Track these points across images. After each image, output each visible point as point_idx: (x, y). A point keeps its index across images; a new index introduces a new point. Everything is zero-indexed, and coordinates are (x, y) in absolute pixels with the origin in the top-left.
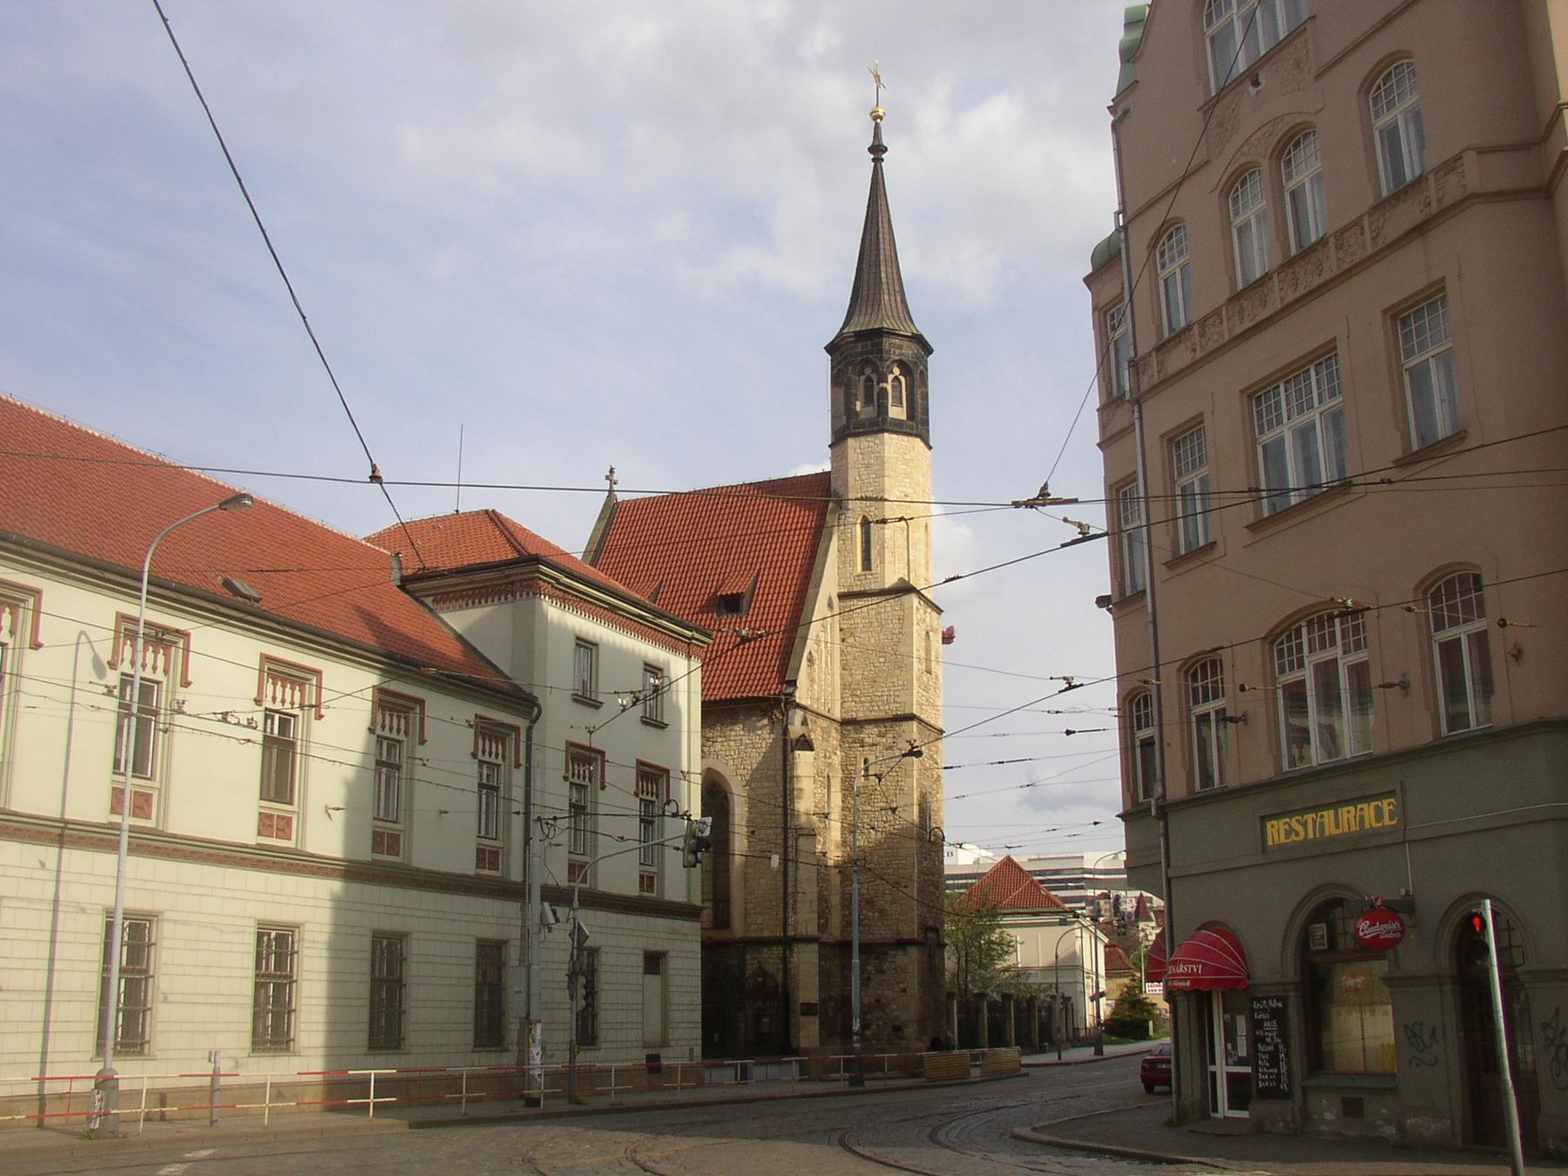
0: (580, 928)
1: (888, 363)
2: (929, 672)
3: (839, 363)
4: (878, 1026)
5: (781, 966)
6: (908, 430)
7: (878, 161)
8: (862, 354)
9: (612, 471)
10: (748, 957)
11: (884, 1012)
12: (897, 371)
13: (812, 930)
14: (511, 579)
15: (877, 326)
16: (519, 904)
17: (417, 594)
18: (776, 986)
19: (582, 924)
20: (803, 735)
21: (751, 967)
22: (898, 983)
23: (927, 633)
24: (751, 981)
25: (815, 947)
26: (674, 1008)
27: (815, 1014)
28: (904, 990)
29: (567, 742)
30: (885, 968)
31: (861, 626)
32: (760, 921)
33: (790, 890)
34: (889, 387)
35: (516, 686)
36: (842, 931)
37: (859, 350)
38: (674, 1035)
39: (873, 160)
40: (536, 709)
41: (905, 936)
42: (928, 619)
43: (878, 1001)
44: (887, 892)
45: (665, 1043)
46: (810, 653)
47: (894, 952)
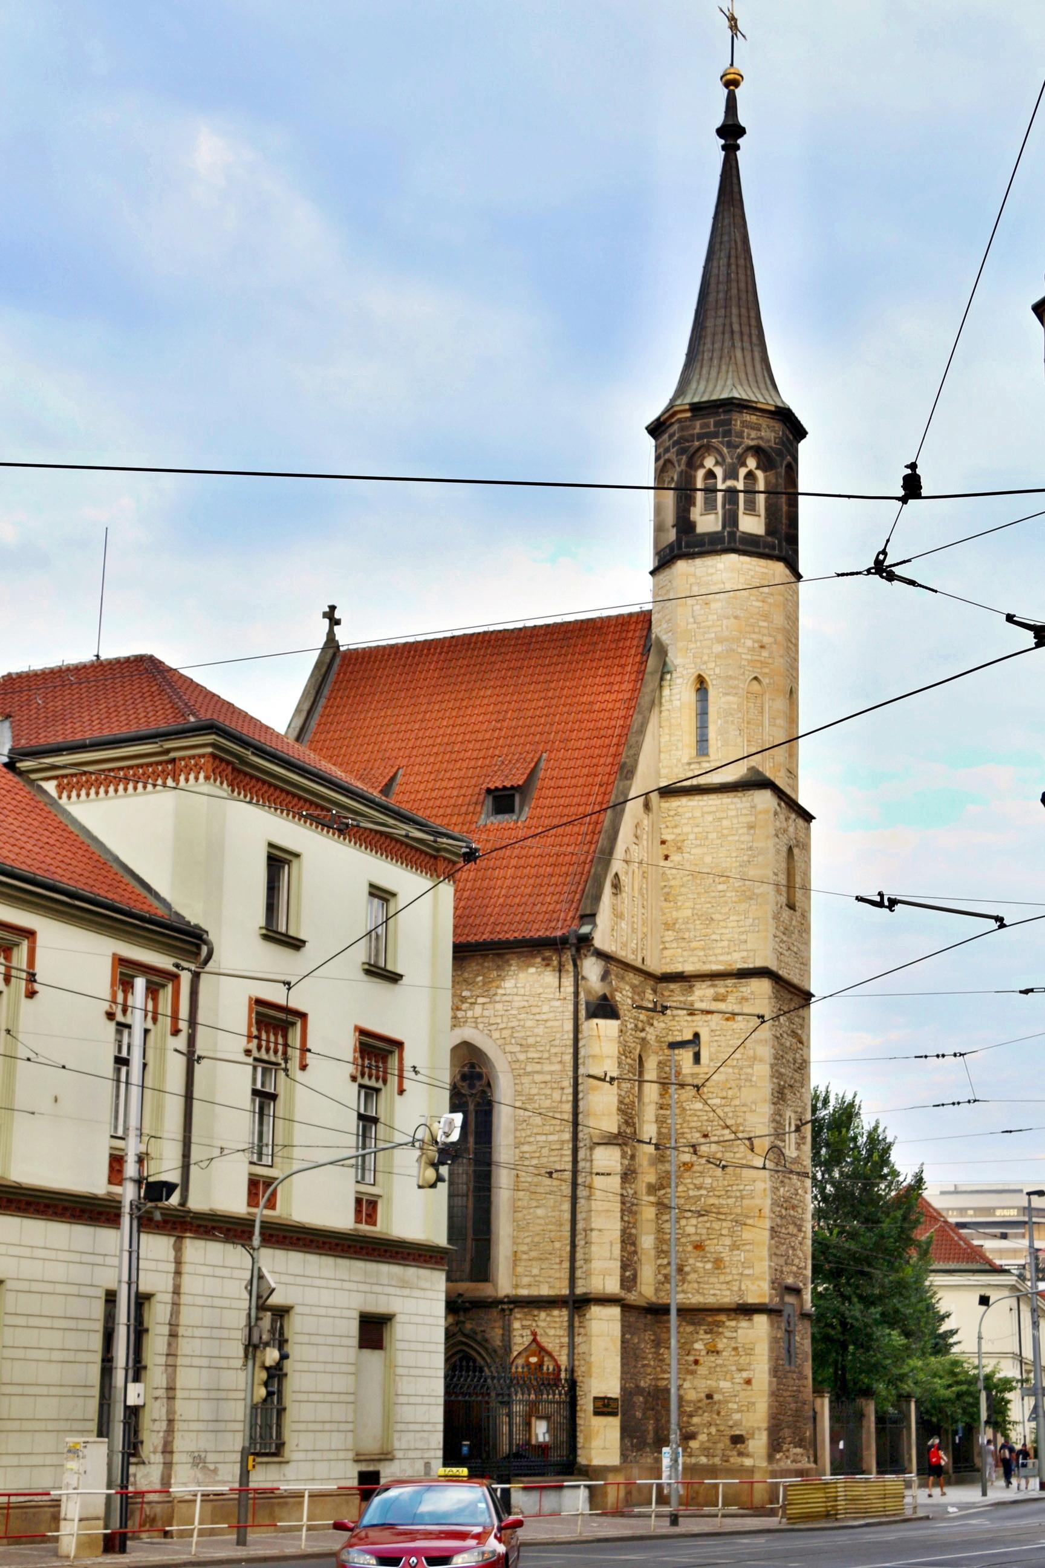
0: (261, 1277)
1: (739, 450)
2: (791, 906)
3: (667, 450)
4: (709, 1434)
5: (565, 1340)
6: (767, 551)
7: (731, 149)
8: (700, 436)
9: (333, 608)
10: (516, 1325)
11: (718, 1413)
12: (752, 463)
13: (612, 1286)
14: (172, 755)
15: (724, 396)
16: (172, 1240)
17: (33, 776)
18: (558, 1367)
19: (265, 1271)
20: (604, 997)
21: (520, 1340)
22: (740, 1370)
23: (790, 850)
24: (520, 1361)
25: (615, 1311)
26: (402, 1399)
27: (613, 1414)
28: (748, 1382)
29: (250, 999)
30: (720, 1346)
31: (691, 837)
32: (535, 1271)
33: (580, 1226)
35: (177, 914)
36: (657, 1290)
37: (697, 431)
38: (400, 1443)
39: (724, 148)
40: (205, 949)
41: (751, 1299)
42: (791, 829)
43: (709, 1396)
44: (724, 1232)
45: (386, 1456)
46: (616, 875)
47: (733, 1323)
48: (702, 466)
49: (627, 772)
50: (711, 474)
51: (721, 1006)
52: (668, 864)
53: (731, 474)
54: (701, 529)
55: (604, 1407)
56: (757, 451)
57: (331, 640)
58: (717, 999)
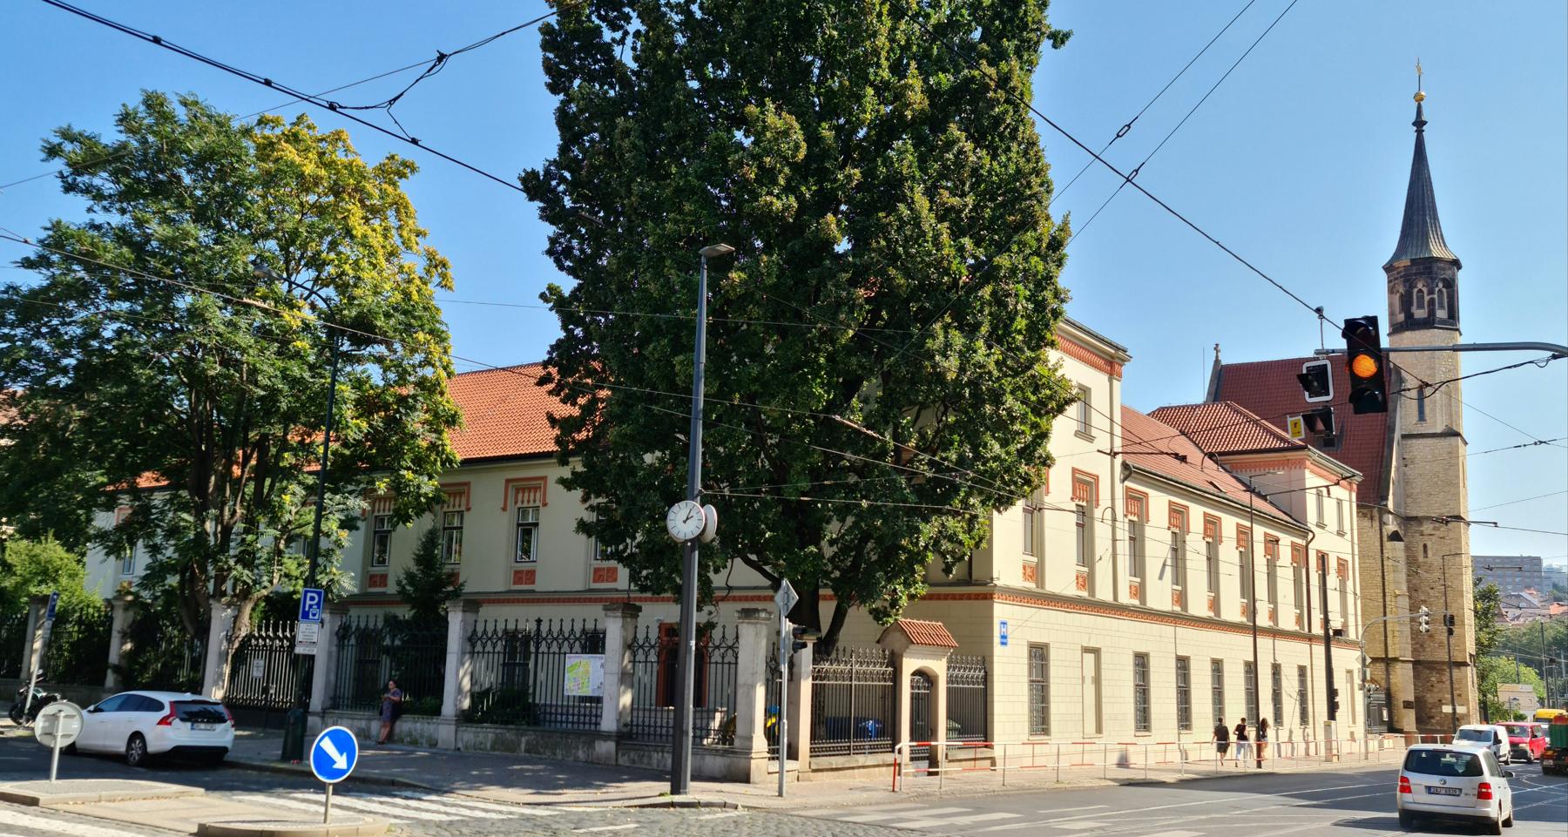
5: (1384, 676)
7: (1420, 133)
9: (1217, 345)
12: (1441, 285)
34: (1436, 296)
40: (1310, 536)
48: (1416, 287)
49: (1391, 429)
50: (1420, 291)
51: (1437, 532)
52: (1406, 469)
53: (1431, 292)
54: (1416, 316)
55: (1407, 705)
56: (1444, 280)
57: (1217, 361)
58: (1434, 529)
